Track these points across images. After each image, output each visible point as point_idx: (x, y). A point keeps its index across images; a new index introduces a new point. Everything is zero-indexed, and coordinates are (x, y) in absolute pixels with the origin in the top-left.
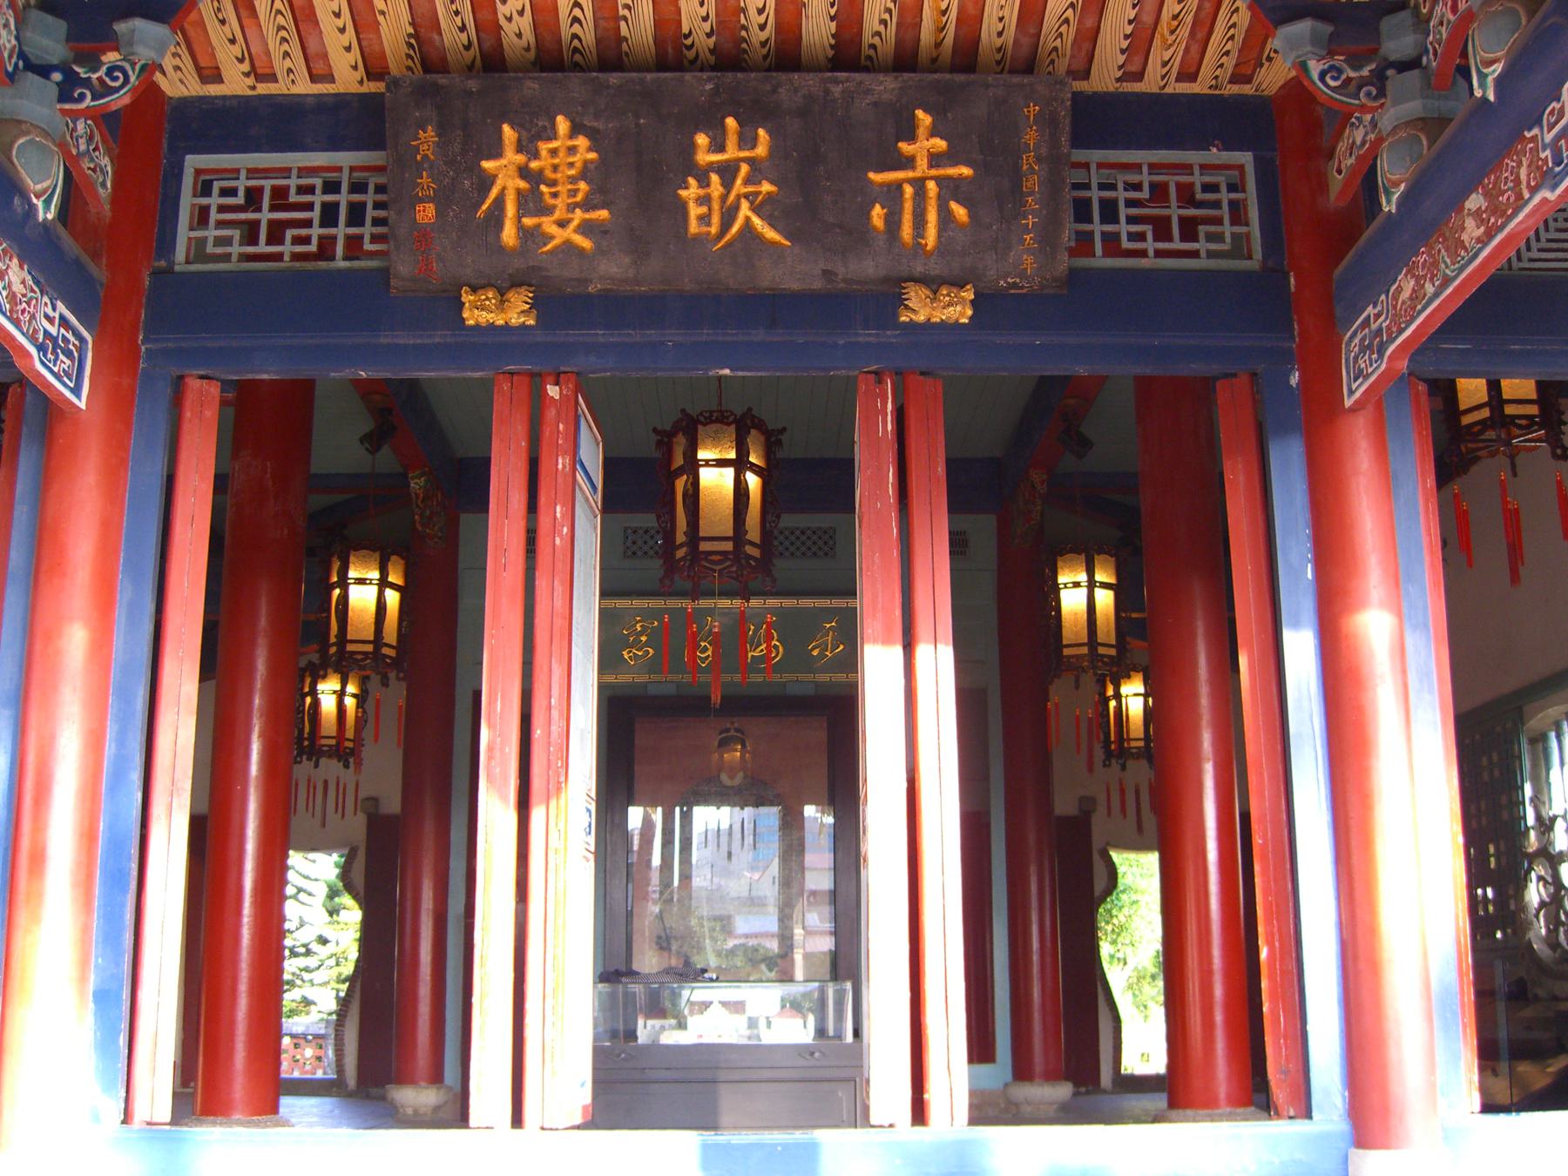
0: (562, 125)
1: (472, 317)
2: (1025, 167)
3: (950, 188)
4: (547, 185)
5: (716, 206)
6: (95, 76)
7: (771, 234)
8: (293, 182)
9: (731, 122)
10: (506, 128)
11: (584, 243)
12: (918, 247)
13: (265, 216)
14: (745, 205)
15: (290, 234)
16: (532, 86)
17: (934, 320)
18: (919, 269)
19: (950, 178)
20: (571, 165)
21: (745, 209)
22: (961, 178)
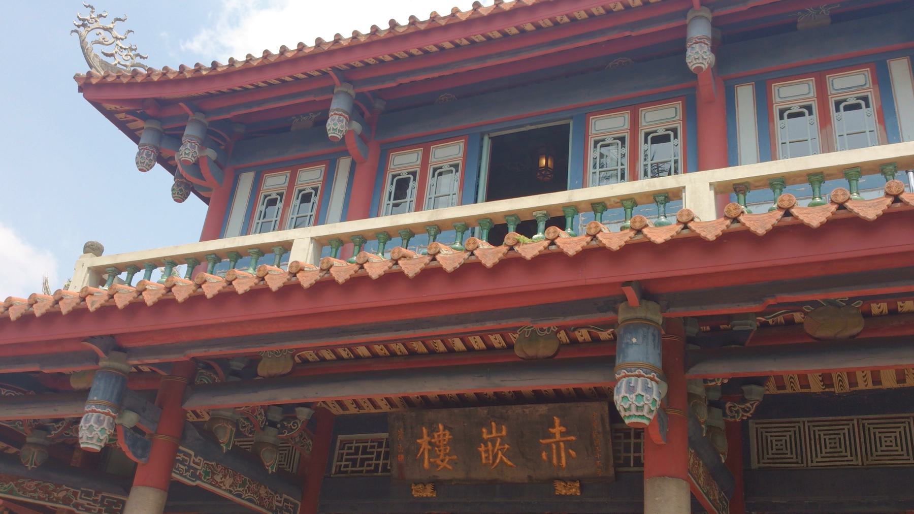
0: (441, 427)
1: (416, 495)
2: (595, 436)
3: (569, 445)
4: (437, 447)
5: (490, 453)
6: (289, 425)
7: (509, 463)
8: (369, 444)
9: (493, 424)
10: (424, 428)
12: (560, 467)
13: (360, 456)
14: (500, 452)
15: (366, 463)
16: (431, 415)
17: (568, 494)
18: (561, 474)
19: (568, 441)
20: (444, 440)
21: (500, 455)
22: (572, 441)
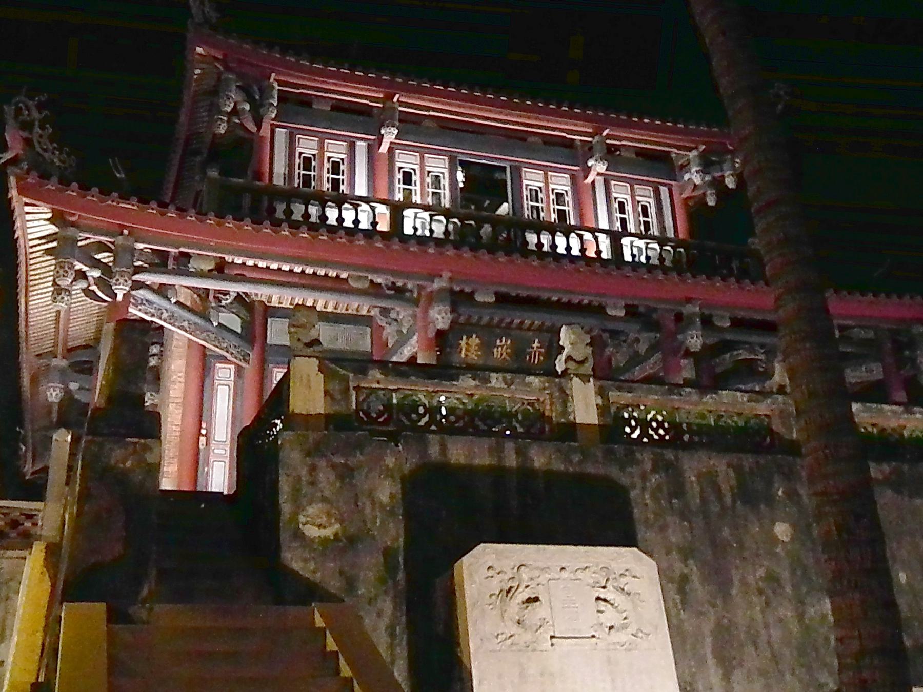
11: (476, 358)
